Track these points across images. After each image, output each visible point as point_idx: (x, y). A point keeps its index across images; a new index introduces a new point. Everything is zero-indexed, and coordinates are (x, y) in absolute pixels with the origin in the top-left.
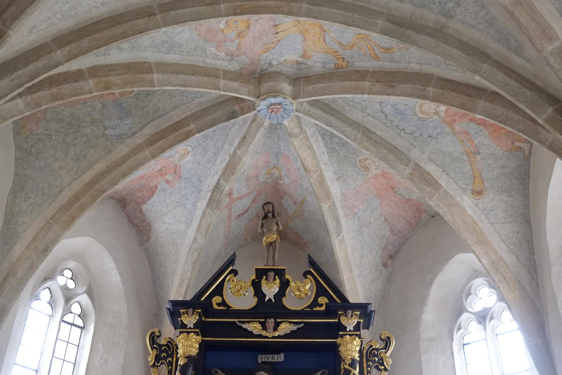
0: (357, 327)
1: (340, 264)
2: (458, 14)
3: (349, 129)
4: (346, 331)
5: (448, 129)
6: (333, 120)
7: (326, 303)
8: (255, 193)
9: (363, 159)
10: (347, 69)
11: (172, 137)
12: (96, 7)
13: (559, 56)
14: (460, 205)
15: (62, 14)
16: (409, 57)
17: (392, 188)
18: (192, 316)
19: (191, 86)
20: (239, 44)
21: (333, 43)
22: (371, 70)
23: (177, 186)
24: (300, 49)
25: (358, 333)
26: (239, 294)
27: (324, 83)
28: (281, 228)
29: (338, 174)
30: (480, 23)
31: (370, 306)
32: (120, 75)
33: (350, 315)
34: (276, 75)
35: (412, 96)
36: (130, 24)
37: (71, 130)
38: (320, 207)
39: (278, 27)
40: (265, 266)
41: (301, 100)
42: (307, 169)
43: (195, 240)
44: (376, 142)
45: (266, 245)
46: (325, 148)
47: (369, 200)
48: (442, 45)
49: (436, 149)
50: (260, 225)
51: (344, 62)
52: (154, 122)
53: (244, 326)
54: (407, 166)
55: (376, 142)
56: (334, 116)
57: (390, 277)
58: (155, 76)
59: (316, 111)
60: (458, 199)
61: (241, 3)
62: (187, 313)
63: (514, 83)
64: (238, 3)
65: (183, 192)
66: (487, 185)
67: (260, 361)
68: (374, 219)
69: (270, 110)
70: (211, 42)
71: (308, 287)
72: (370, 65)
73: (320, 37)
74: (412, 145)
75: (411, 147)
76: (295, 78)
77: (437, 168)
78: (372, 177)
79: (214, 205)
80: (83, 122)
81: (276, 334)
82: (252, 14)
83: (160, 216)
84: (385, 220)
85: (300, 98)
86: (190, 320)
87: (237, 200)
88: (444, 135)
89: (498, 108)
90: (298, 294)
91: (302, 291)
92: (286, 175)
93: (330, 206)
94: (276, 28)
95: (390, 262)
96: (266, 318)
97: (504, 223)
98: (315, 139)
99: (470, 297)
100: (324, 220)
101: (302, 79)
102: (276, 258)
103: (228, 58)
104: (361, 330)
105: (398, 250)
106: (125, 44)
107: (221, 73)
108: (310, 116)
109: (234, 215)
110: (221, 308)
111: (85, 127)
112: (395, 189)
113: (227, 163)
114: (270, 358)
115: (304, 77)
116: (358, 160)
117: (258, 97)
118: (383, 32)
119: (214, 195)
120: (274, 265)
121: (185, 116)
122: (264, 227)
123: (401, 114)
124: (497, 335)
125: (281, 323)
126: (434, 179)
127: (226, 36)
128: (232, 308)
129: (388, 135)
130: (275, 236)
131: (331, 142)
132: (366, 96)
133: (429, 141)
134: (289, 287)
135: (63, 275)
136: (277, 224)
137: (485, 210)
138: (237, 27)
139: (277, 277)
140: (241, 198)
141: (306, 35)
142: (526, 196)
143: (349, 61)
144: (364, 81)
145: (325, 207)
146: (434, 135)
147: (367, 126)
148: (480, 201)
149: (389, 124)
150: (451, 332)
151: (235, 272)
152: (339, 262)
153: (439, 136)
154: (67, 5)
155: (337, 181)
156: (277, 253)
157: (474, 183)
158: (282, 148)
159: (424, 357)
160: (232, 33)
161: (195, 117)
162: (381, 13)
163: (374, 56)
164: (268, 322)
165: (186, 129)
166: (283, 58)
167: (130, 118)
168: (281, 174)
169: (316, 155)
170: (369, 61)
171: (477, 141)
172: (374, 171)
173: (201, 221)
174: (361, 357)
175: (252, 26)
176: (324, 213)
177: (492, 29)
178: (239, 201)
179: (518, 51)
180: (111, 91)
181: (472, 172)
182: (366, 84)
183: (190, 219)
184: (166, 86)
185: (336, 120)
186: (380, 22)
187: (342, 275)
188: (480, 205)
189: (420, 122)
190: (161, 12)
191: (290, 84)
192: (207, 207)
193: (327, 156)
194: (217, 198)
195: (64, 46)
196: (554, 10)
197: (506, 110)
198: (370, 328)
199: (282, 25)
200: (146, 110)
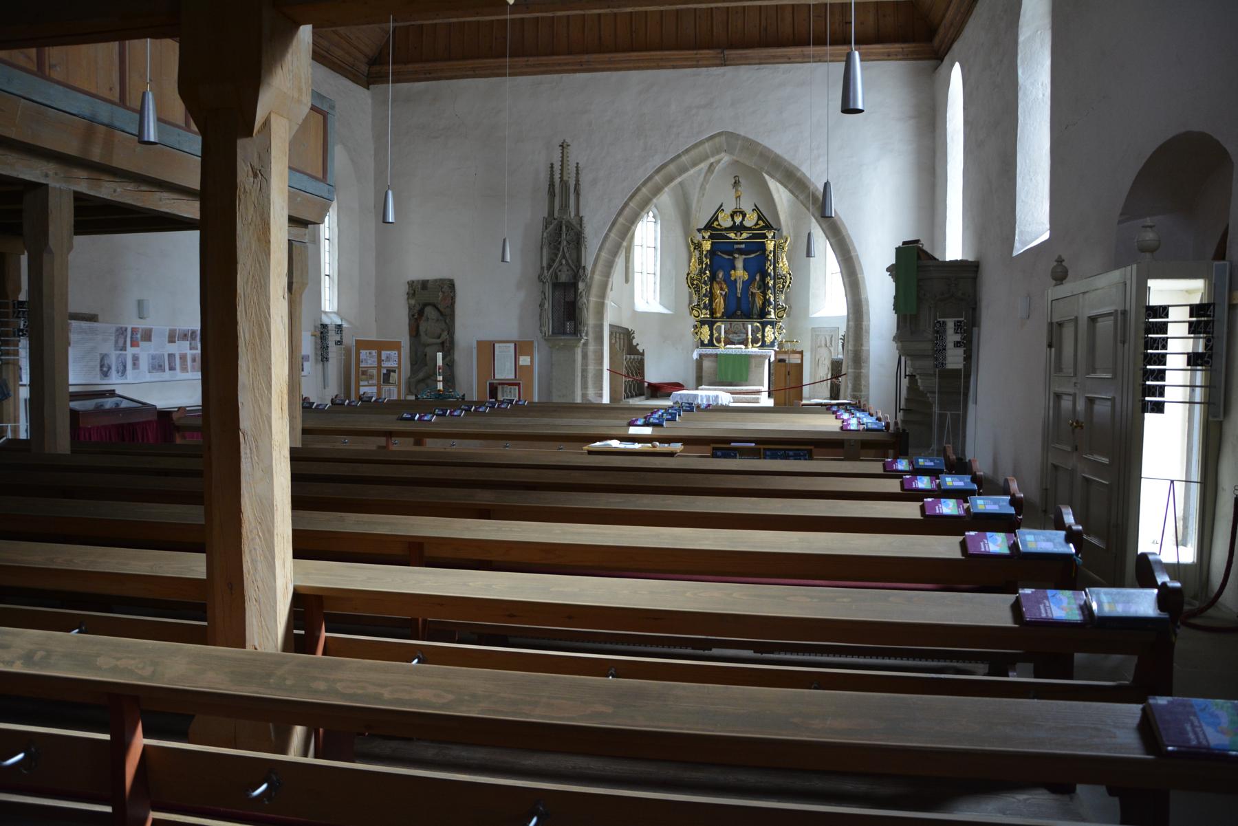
53: (728, 235)
86: (707, 235)
114: (739, 246)
151: (723, 210)
174: (775, 249)
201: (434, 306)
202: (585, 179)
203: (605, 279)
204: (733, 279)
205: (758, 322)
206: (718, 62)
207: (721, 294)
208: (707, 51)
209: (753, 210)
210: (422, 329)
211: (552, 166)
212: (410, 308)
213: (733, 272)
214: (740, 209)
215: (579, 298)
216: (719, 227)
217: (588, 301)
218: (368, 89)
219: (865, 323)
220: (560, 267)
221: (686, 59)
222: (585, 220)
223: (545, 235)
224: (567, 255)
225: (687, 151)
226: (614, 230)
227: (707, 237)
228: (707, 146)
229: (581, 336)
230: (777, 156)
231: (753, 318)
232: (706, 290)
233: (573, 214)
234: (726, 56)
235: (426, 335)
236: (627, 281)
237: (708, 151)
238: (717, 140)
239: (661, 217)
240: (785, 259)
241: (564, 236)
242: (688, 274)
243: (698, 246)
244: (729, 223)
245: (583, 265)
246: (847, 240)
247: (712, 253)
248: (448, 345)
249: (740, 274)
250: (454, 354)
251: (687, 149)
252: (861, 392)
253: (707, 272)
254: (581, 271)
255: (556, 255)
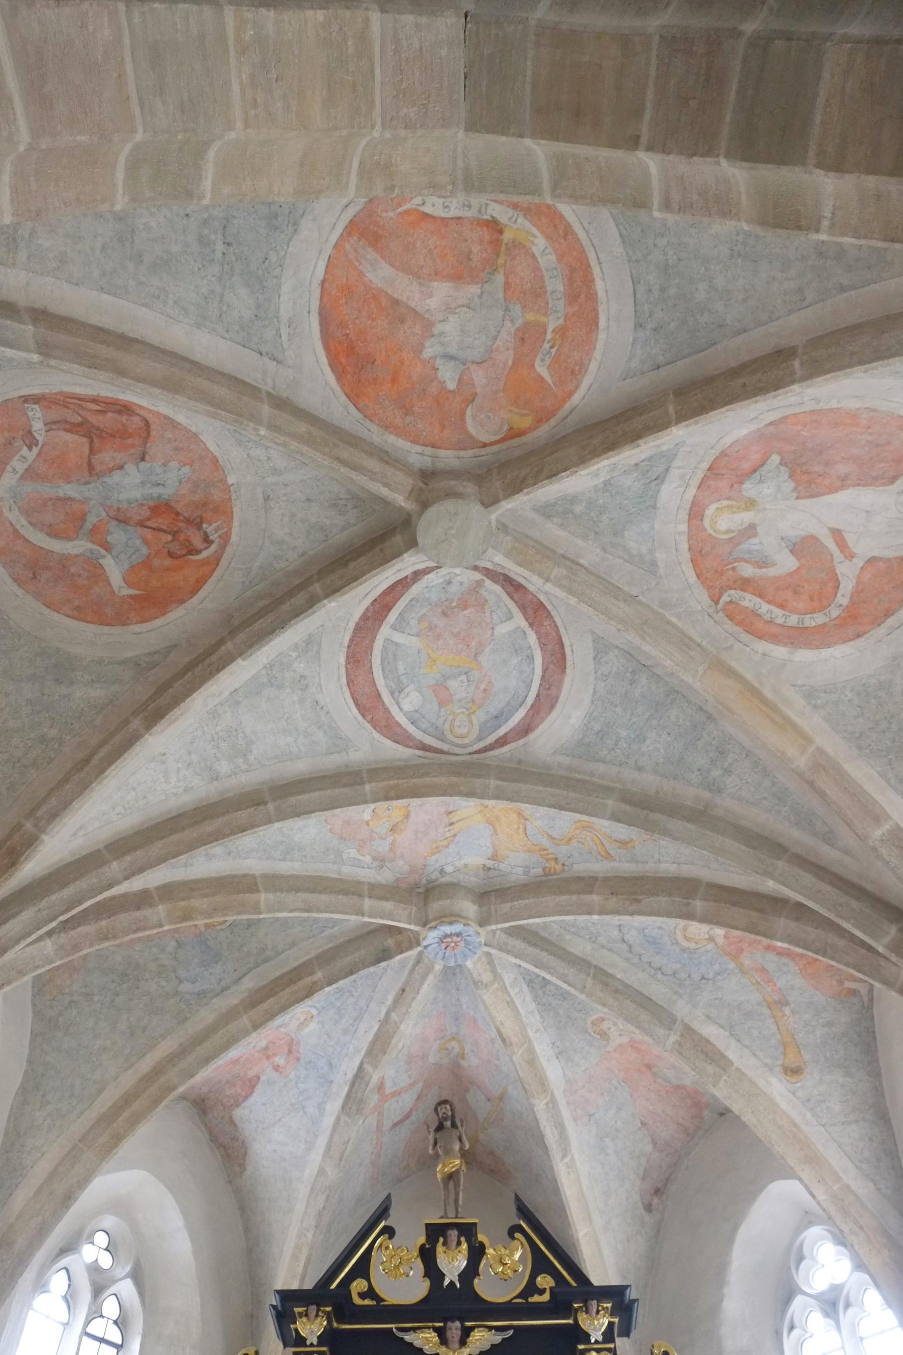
0: (609, 1336)
1: (570, 1208)
2: (729, 787)
3: (572, 970)
4: (588, 1342)
5: (732, 965)
6: (544, 956)
7: (551, 1288)
8: (421, 1084)
9: (597, 1019)
10: (564, 875)
11: (285, 994)
12: (176, 794)
13: (893, 845)
14: (765, 1094)
15: (124, 807)
16: (660, 853)
17: (649, 1067)
18: (315, 1320)
19: (319, 911)
20: (393, 844)
21: (540, 836)
22: (601, 875)
23: (292, 1076)
24: (488, 847)
25: (612, 1346)
26: (398, 1273)
27: (528, 898)
28: (467, 1147)
29: (558, 1047)
30: (765, 798)
31: (629, 1289)
32: (206, 896)
33: (595, 1310)
34: (450, 889)
35: (669, 915)
36: (227, 817)
37: (125, 986)
38: (532, 1106)
39: (453, 814)
40: (442, 1217)
41: (493, 927)
42: (507, 1040)
43: (321, 1172)
44: (617, 991)
45: (443, 1179)
46: (534, 1003)
47: (613, 1090)
48: (709, 833)
49: (716, 999)
50: (432, 1142)
51: (557, 864)
52: (258, 969)
53: (408, 1337)
54: (670, 1029)
55: (617, 991)
56: (547, 951)
57: (658, 1230)
58: (263, 896)
59: (518, 944)
60: (761, 1083)
61: (396, 781)
62: (307, 1315)
63: (829, 888)
64: (392, 782)
65: (301, 1086)
66: (806, 1056)
68: (623, 1123)
69: (444, 946)
70: (350, 840)
71: (517, 1256)
72: (599, 867)
73: (519, 828)
74: (676, 993)
75: (675, 997)
76: (482, 891)
77: (721, 1031)
78: (615, 1050)
79: (355, 1108)
80: (145, 971)
82: (412, 798)
83: (264, 1129)
84: (643, 1124)
85: (490, 925)
87: (392, 1097)
88: (726, 975)
89: (810, 929)
90: (500, 1270)
91: (507, 1264)
92: (472, 1051)
93: (547, 1104)
94: (451, 816)
95: (655, 1201)
96: (445, 1320)
97: (844, 1123)
98: (517, 990)
99: (804, 1264)
100: (539, 1127)
101: (493, 893)
102: (460, 1203)
103: (376, 864)
104: (617, 1339)
105: (668, 1179)
106: (217, 849)
107: (366, 888)
108: (508, 952)
109: (387, 1123)
110: (367, 1302)
111: (147, 980)
112: (655, 1070)
113: (376, 1034)
115: (496, 891)
116: (589, 1021)
117: (424, 925)
118: (616, 818)
119: (354, 1090)
120: (457, 1217)
121: (308, 957)
122: (438, 1145)
123: (654, 943)
124: (861, 1339)
125: (472, 1329)
126: (718, 1049)
127: (372, 831)
128: (385, 1301)
129: (635, 978)
130: (457, 1162)
131: (544, 993)
132: (595, 917)
133: (702, 986)
134: (485, 1257)
135: (92, 1243)
136: (460, 1139)
137: (809, 1100)
138: (390, 817)
139: (463, 1239)
140: (399, 1093)
141: (497, 825)
142: (875, 1074)
143: (566, 863)
144: (591, 893)
145: (540, 1105)
146: (711, 975)
147: (601, 965)
148: (799, 1085)
149: (636, 960)
150: (778, 1335)
152: (568, 1205)
153: (719, 977)
154: (133, 793)
155: (557, 1058)
156: (461, 1193)
157: (785, 1054)
158: (465, 1006)
160: (382, 827)
161: (325, 958)
162: (609, 790)
163: (603, 853)
164: (450, 1329)
165: (308, 980)
166: (463, 862)
167: (220, 964)
168: (464, 1050)
169: (520, 1014)
170: (597, 862)
171: (781, 983)
172: (617, 1039)
173: (332, 1135)
175: (413, 815)
176: (538, 1117)
177: (785, 806)
178: (395, 1098)
179: (829, 838)
180: (192, 923)
181: (778, 1036)
182: (595, 898)
183: (314, 1133)
184: (279, 911)
185: (550, 957)
186: (610, 802)
187: (576, 1230)
188: (800, 1093)
189: (685, 956)
190: (274, 800)
191: (474, 902)
192: (343, 1112)
193: (538, 1017)
194: (359, 1095)
195: (123, 855)
196: (876, 774)
197: (823, 933)
198: (631, 1335)
199: (459, 812)
200: (245, 949)
209: (513, 1231)
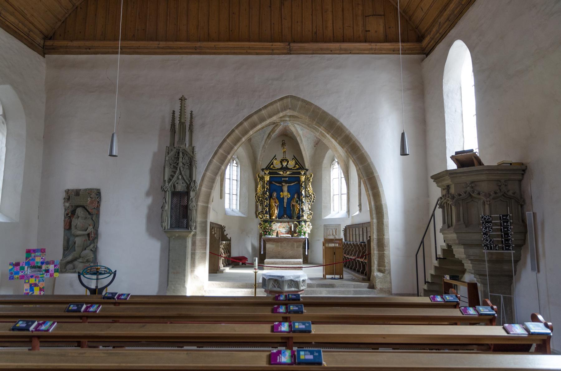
53: (279, 173)
54: (318, 132)
55: (310, 127)
67: (283, 180)
81: (286, 174)
86: (267, 172)
95: (316, 145)
114: (285, 179)
120: (285, 158)
145: (298, 139)
151: (276, 159)
159: (323, 172)
174: (305, 180)
191: (288, 118)
201: (84, 207)
202: (197, 122)
203: (209, 190)
204: (282, 197)
205: (296, 221)
206: (285, 51)
207: (275, 205)
208: (279, 44)
209: (293, 159)
210: (73, 224)
211: (174, 112)
212: (65, 210)
213: (281, 193)
214: (285, 158)
215: (190, 202)
216: (274, 168)
217: (197, 205)
218: (44, 57)
219: (385, 220)
220: (178, 181)
221: (266, 49)
222: (196, 150)
223: (167, 159)
224: (183, 173)
225: (266, 107)
226: (216, 158)
227: (267, 173)
228: (278, 104)
229: (191, 229)
230: (324, 112)
231: (293, 219)
232: (267, 203)
233: (187, 145)
234: (291, 48)
235: (76, 228)
236: (221, 197)
237: (279, 108)
238: (285, 101)
239: (240, 163)
240: (311, 186)
241: (181, 159)
242: (256, 194)
243: (262, 178)
244: (280, 166)
245: (194, 179)
246: (371, 166)
247: (270, 182)
248: (93, 235)
249: (285, 194)
250: (97, 242)
251: (265, 106)
252: (385, 267)
253: (268, 193)
254: (192, 184)
255: (175, 172)
